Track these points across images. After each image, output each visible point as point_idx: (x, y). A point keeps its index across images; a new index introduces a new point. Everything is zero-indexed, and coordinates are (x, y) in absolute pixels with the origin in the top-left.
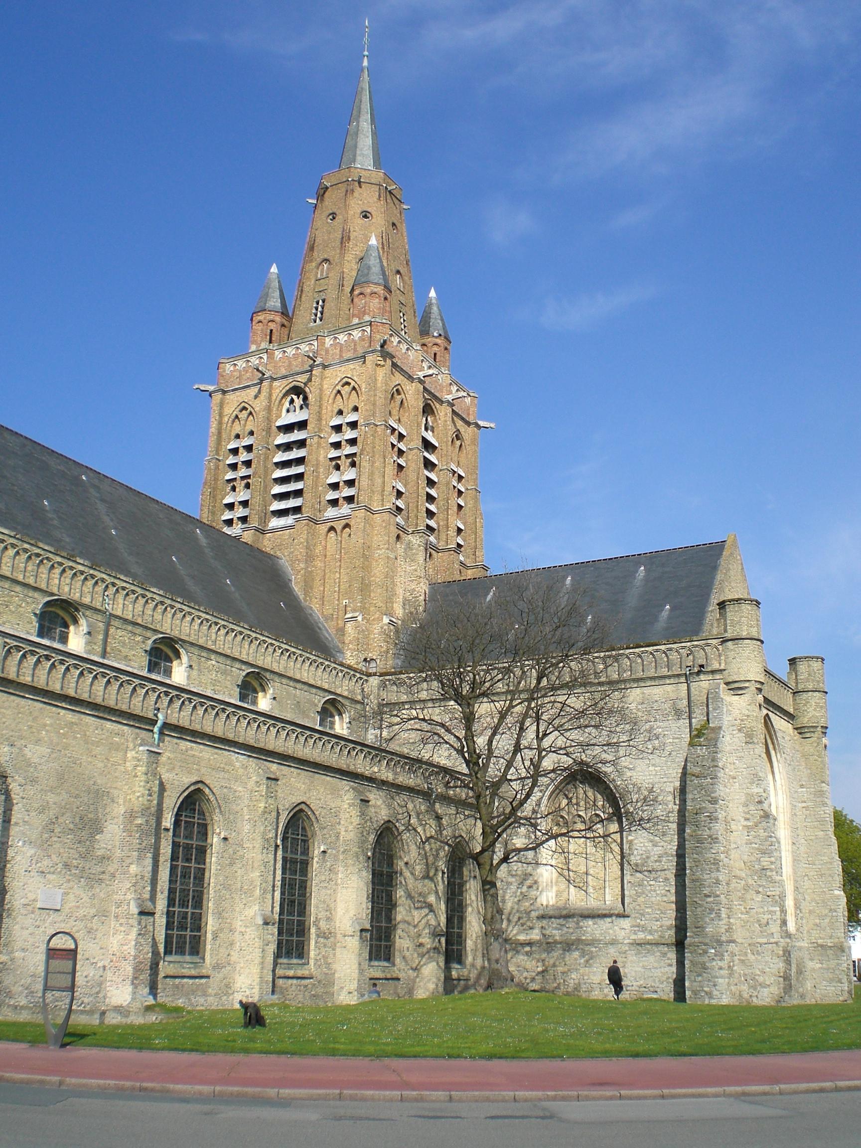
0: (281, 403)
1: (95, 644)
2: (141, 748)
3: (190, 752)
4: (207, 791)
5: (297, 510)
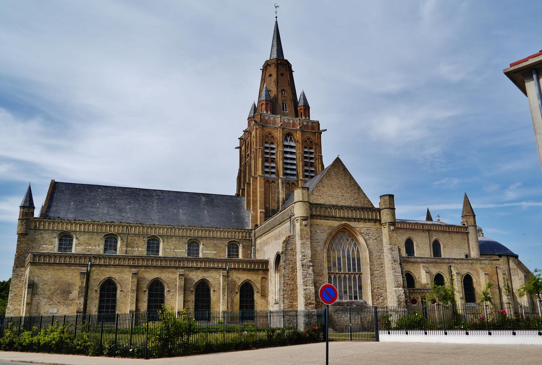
3: (105, 270)
4: (113, 279)
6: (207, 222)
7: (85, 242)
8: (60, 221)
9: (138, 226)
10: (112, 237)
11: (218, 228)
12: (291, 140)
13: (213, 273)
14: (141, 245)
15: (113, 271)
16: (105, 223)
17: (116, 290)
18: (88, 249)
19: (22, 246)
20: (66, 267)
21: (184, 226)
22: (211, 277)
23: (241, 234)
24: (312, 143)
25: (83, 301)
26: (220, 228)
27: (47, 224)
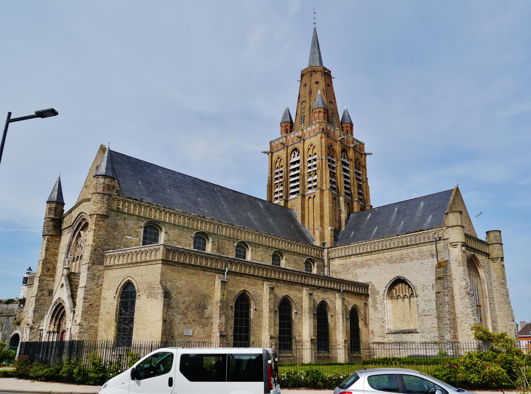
0: (291, 155)
1: (215, 245)
2: (219, 280)
4: (247, 293)
5: (298, 192)
7: (175, 239)
8: (148, 204)
10: (201, 237)
13: (330, 294)
14: (231, 251)
15: (248, 283)
16: (197, 217)
19: (101, 233)
20: (201, 272)
21: (270, 235)
26: (300, 242)
27: (132, 207)
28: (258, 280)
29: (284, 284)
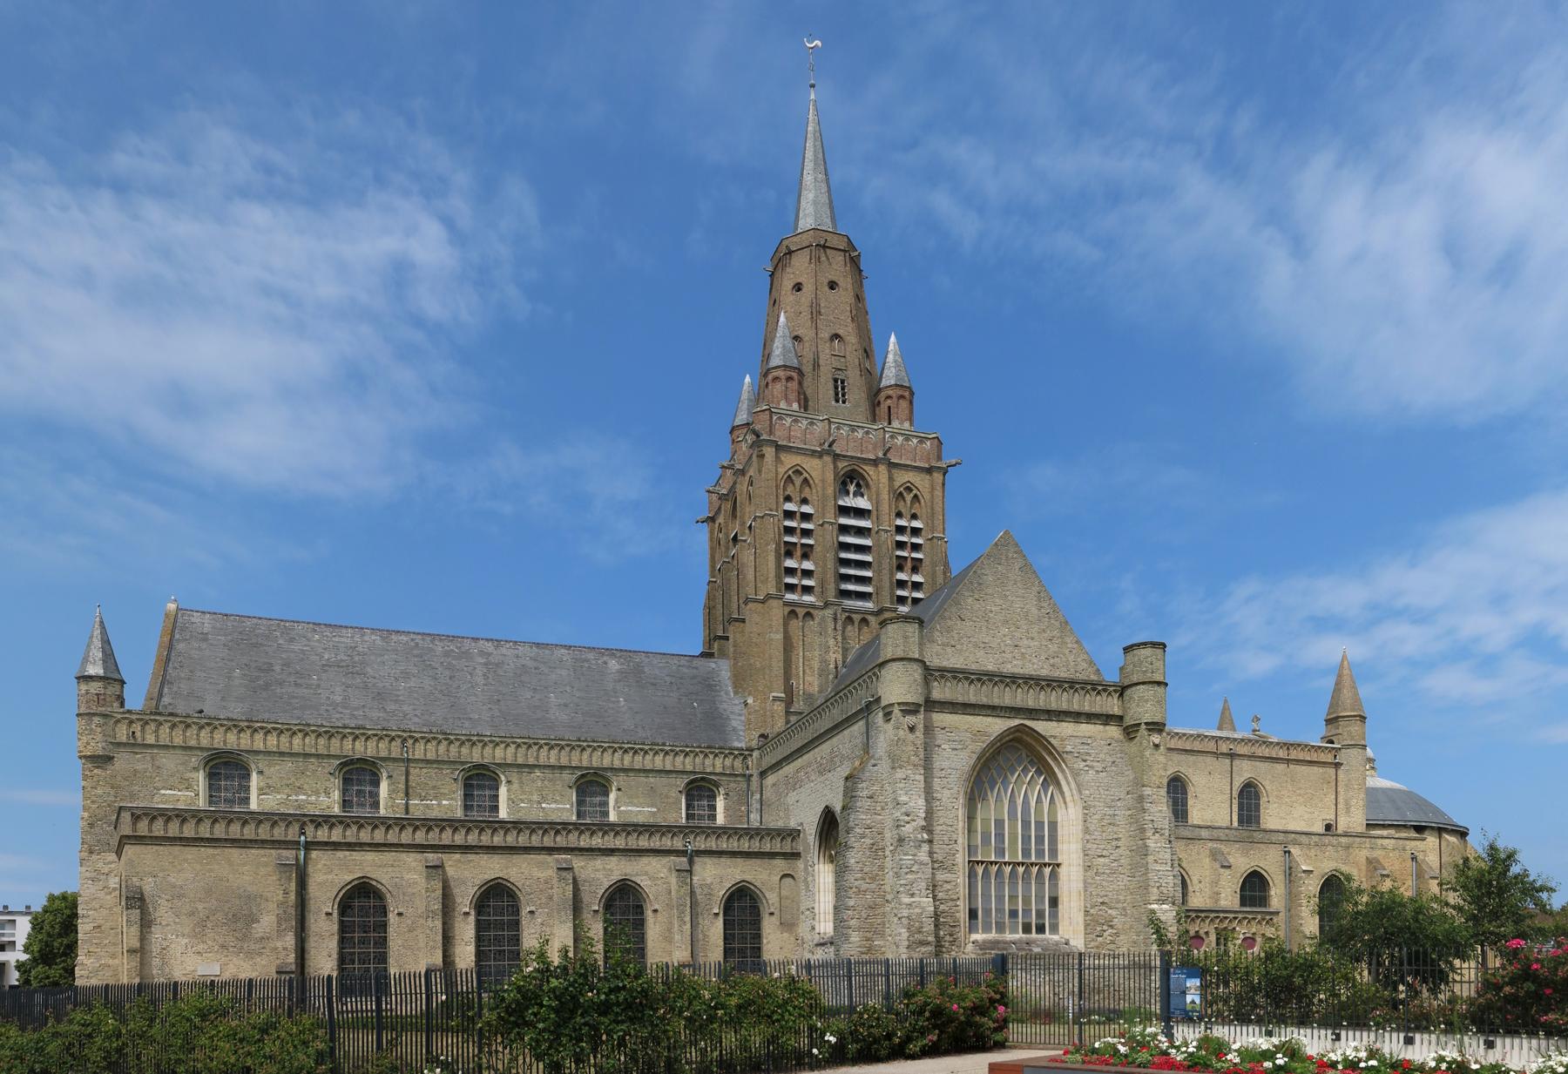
1: (399, 783)
4: (374, 883)
6: (626, 727)
7: (285, 782)
9: (434, 738)
10: (364, 769)
11: (658, 745)
12: (858, 493)
17: (384, 911)
18: (297, 801)
22: (646, 874)
23: (721, 760)
24: (919, 502)
25: (293, 942)
26: (664, 744)
28: (407, 854)
29: (490, 855)
